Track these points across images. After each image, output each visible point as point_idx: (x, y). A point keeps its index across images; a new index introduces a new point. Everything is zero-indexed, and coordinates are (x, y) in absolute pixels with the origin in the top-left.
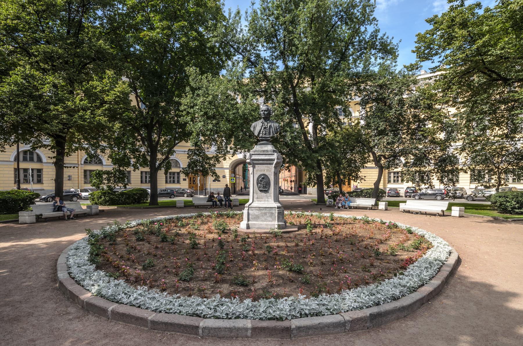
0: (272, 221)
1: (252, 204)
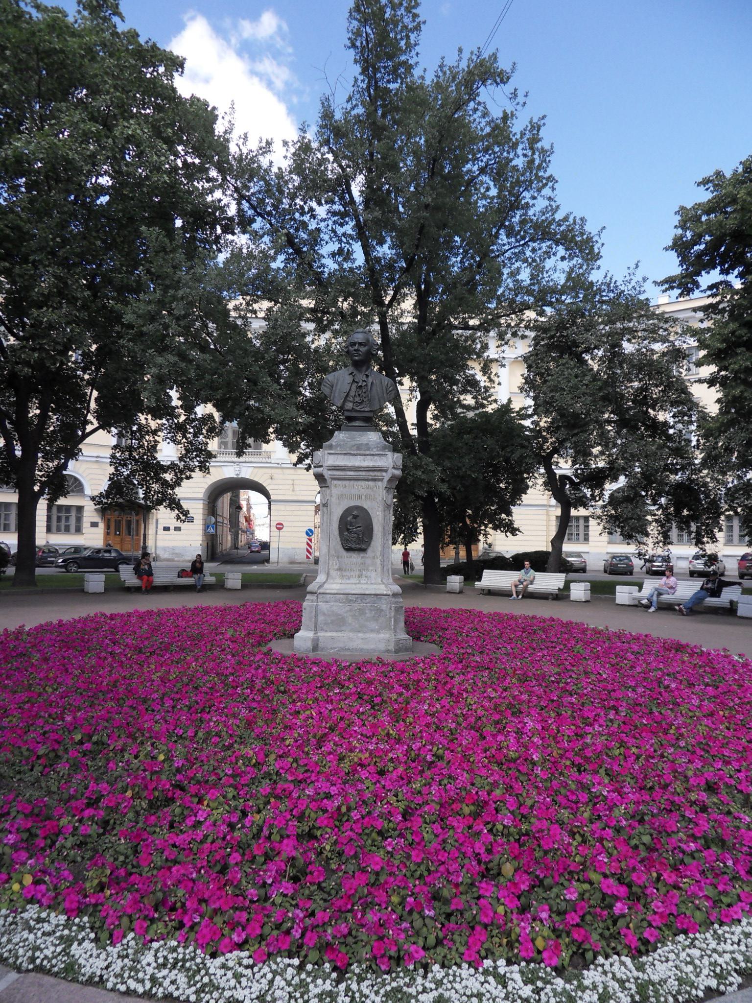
0: (378, 632)
1: (326, 586)
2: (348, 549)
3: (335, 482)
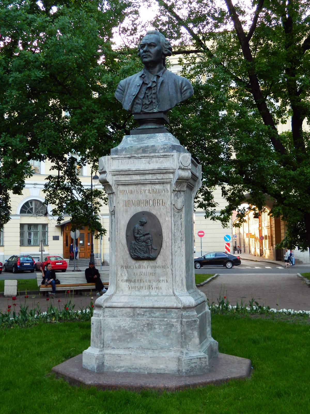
1: (114, 299)
2: (137, 259)
3: (121, 188)
